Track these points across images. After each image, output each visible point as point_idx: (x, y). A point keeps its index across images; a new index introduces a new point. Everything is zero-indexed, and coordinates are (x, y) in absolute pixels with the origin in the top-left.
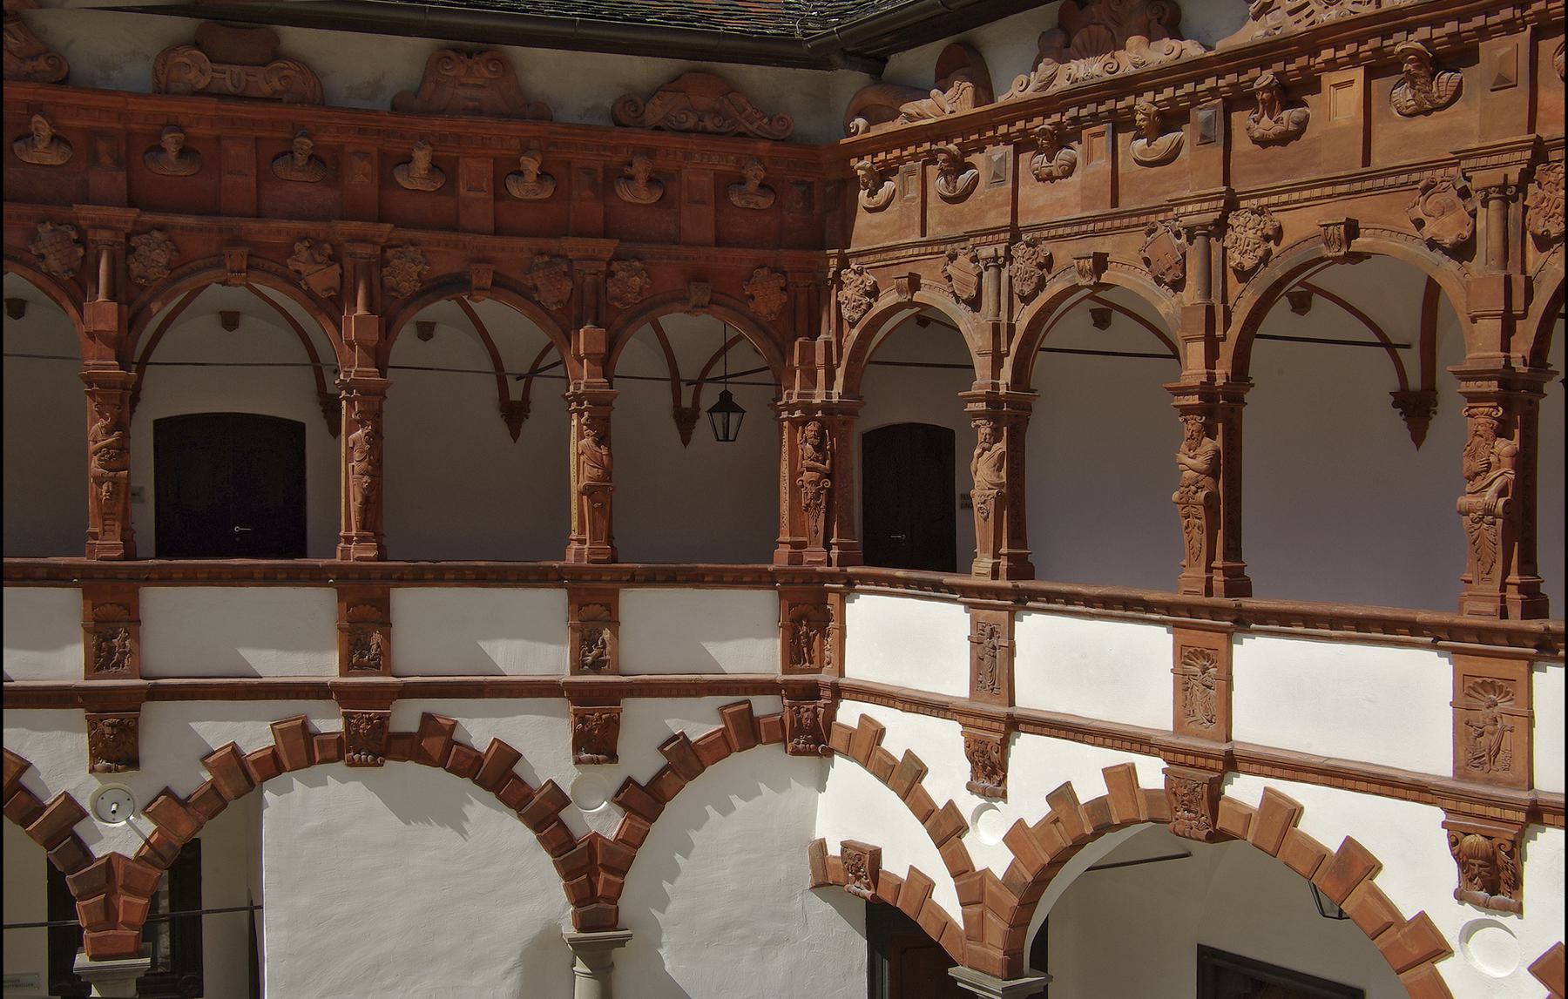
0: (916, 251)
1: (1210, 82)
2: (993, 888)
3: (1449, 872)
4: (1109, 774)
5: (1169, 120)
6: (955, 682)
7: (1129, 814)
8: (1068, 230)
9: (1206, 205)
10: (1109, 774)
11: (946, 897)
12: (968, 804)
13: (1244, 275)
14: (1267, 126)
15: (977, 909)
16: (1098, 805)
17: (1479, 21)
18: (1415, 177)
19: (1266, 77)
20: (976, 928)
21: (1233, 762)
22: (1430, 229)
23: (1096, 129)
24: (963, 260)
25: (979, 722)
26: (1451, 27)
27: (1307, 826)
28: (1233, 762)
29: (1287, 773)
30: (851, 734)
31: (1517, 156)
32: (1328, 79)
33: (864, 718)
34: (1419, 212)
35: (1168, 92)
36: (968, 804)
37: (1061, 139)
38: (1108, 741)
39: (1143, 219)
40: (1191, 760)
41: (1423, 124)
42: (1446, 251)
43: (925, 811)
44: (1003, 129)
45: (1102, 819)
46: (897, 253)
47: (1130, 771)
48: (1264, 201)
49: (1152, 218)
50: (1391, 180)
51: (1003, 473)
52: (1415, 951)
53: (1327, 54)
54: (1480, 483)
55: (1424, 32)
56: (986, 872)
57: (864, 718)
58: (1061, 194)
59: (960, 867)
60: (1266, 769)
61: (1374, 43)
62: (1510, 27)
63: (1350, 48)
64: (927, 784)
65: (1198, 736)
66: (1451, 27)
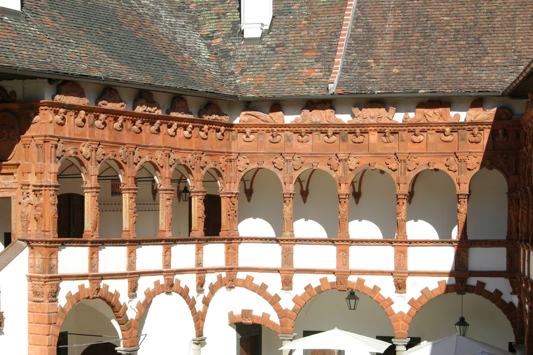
0: (263, 155)
1: (346, 129)
2: (290, 312)
4: (321, 280)
7: (326, 288)
8: (309, 155)
9: (345, 155)
10: (321, 280)
11: (275, 318)
13: (351, 170)
14: (357, 140)
15: (284, 319)
16: (319, 287)
17: (400, 128)
18: (387, 155)
20: (282, 324)
21: (352, 272)
22: (390, 166)
23: (316, 133)
24: (279, 159)
25: (287, 272)
26: (395, 128)
27: (366, 284)
28: (352, 272)
29: (362, 274)
30: (244, 281)
31: (406, 155)
32: (370, 133)
34: (388, 163)
35: (336, 129)
38: (321, 272)
39: (328, 155)
40: (342, 273)
41: (387, 145)
42: (392, 170)
43: (267, 297)
44: (292, 129)
45: (319, 290)
46: (257, 155)
48: (357, 155)
49: (330, 155)
50: (383, 155)
51: (291, 212)
52: (388, 304)
53: (371, 128)
54: (400, 215)
55: (390, 128)
56: (287, 309)
57: (248, 276)
58: (305, 146)
60: (358, 273)
61: (380, 128)
63: (375, 128)
64: (268, 290)
65: (342, 268)
66: (395, 128)
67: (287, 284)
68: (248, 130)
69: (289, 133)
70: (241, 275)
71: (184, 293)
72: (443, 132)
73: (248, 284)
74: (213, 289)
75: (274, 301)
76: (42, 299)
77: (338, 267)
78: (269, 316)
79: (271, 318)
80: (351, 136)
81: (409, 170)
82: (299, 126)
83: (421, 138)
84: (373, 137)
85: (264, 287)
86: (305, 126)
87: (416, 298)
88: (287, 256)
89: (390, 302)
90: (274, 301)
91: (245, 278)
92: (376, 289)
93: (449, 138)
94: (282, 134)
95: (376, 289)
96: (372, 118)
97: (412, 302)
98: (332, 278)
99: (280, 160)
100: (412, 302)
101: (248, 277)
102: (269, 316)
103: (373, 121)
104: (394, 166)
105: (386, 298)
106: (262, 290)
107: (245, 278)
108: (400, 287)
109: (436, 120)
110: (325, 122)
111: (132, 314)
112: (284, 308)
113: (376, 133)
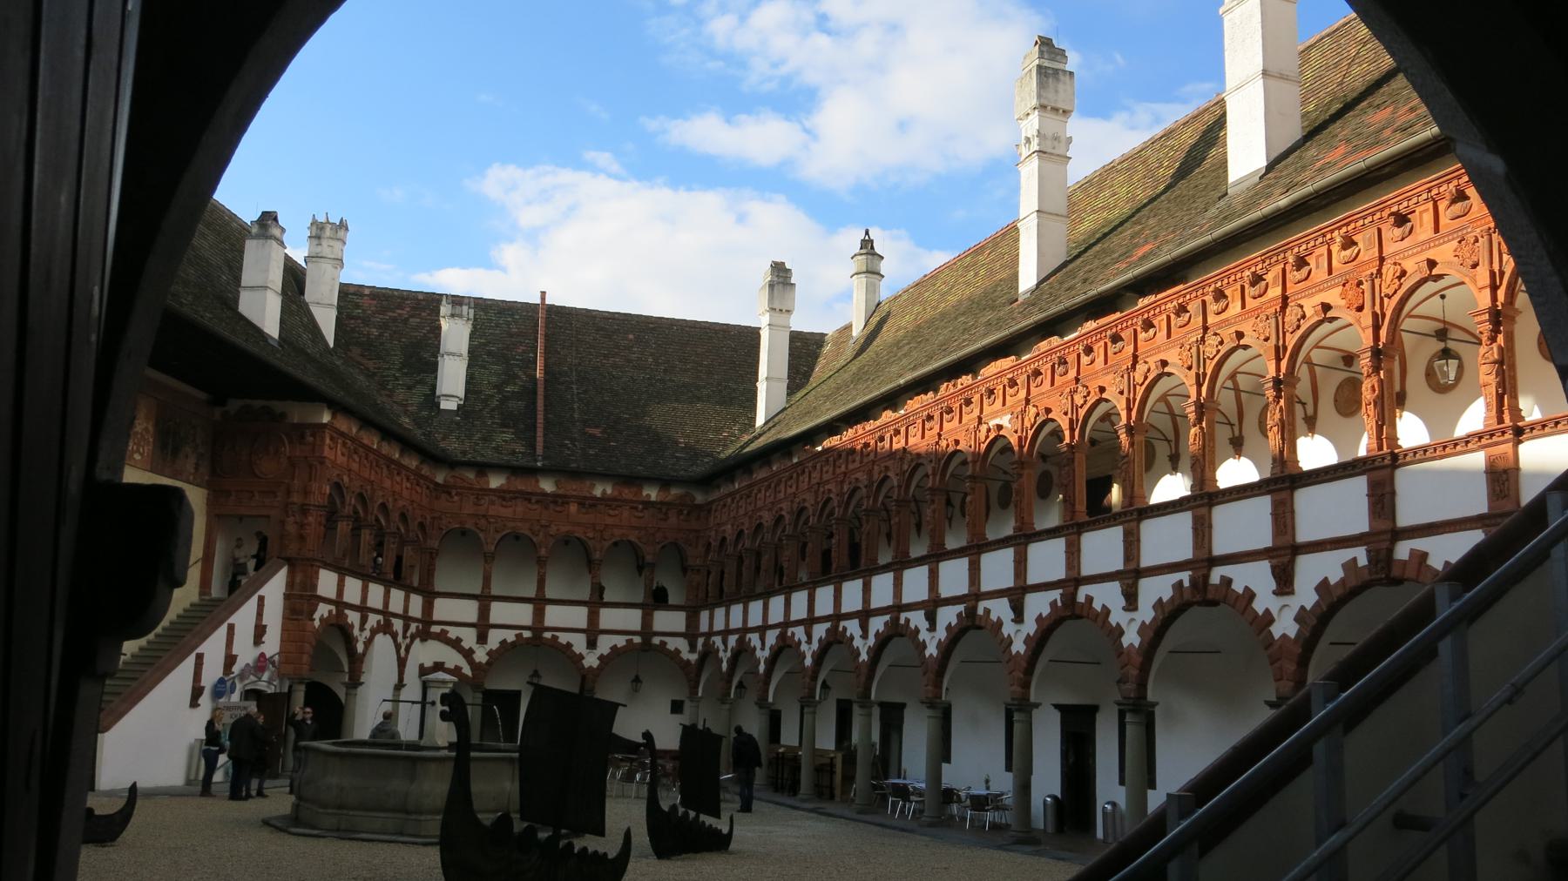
3: (585, 645)
5: (537, 502)
6: (473, 618)
11: (467, 670)
12: (475, 647)
13: (552, 536)
14: (558, 509)
19: (560, 501)
22: (588, 535)
32: (571, 504)
33: (442, 630)
36: (475, 647)
37: (511, 499)
47: (521, 634)
56: (480, 663)
59: (471, 662)
62: (602, 504)
67: (482, 639)
68: (454, 492)
69: (494, 498)
70: (436, 629)
71: (394, 636)
72: (636, 508)
73: (442, 638)
74: (413, 638)
75: (468, 654)
76: (300, 617)
77: (533, 623)
78: (462, 668)
79: (463, 671)
80: (552, 506)
81: (605, 540)
82: (504, 492)
83: (617, 512)
84: (573, 508)
85: (459, 640)
86: (510, 492)
87: (605, 654)
88: (484, 612)
89: (581, 657)
90: (468, 654)
91: (439, 631)
92: (569, 645)
93: (641, 514)
94: (487, 498)
95: (569, 645)
96: (575, 490)
97: (601, 658)
98: (527, 634)
99: (483, 521)
100: (601, 658)
101: (442, 630)
102: (462, 668)
103: (574, 493)
104: (591, 535)
105: (578, 653)
106: (456, 644)
107: (439, 631)
108: (592, 644)
109: (630, 497)
110: (530, 491)
111: (360, 648)
112: (477, 660)
113: (576, 505)
